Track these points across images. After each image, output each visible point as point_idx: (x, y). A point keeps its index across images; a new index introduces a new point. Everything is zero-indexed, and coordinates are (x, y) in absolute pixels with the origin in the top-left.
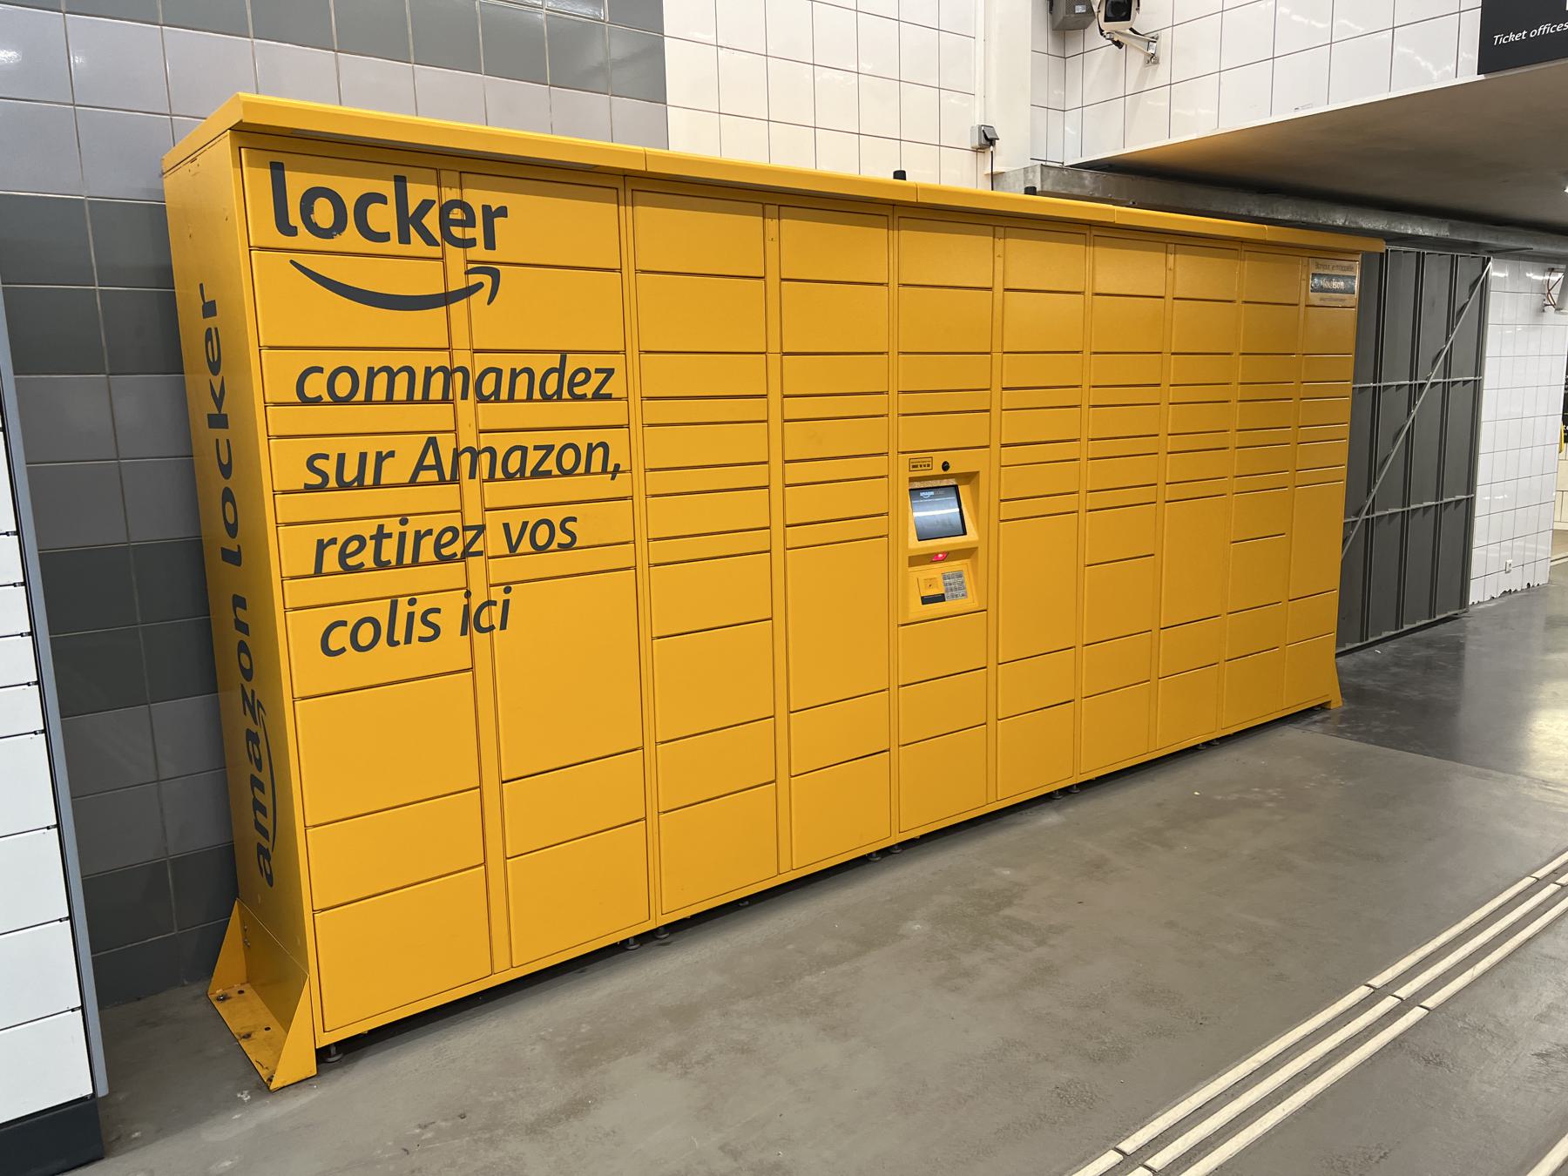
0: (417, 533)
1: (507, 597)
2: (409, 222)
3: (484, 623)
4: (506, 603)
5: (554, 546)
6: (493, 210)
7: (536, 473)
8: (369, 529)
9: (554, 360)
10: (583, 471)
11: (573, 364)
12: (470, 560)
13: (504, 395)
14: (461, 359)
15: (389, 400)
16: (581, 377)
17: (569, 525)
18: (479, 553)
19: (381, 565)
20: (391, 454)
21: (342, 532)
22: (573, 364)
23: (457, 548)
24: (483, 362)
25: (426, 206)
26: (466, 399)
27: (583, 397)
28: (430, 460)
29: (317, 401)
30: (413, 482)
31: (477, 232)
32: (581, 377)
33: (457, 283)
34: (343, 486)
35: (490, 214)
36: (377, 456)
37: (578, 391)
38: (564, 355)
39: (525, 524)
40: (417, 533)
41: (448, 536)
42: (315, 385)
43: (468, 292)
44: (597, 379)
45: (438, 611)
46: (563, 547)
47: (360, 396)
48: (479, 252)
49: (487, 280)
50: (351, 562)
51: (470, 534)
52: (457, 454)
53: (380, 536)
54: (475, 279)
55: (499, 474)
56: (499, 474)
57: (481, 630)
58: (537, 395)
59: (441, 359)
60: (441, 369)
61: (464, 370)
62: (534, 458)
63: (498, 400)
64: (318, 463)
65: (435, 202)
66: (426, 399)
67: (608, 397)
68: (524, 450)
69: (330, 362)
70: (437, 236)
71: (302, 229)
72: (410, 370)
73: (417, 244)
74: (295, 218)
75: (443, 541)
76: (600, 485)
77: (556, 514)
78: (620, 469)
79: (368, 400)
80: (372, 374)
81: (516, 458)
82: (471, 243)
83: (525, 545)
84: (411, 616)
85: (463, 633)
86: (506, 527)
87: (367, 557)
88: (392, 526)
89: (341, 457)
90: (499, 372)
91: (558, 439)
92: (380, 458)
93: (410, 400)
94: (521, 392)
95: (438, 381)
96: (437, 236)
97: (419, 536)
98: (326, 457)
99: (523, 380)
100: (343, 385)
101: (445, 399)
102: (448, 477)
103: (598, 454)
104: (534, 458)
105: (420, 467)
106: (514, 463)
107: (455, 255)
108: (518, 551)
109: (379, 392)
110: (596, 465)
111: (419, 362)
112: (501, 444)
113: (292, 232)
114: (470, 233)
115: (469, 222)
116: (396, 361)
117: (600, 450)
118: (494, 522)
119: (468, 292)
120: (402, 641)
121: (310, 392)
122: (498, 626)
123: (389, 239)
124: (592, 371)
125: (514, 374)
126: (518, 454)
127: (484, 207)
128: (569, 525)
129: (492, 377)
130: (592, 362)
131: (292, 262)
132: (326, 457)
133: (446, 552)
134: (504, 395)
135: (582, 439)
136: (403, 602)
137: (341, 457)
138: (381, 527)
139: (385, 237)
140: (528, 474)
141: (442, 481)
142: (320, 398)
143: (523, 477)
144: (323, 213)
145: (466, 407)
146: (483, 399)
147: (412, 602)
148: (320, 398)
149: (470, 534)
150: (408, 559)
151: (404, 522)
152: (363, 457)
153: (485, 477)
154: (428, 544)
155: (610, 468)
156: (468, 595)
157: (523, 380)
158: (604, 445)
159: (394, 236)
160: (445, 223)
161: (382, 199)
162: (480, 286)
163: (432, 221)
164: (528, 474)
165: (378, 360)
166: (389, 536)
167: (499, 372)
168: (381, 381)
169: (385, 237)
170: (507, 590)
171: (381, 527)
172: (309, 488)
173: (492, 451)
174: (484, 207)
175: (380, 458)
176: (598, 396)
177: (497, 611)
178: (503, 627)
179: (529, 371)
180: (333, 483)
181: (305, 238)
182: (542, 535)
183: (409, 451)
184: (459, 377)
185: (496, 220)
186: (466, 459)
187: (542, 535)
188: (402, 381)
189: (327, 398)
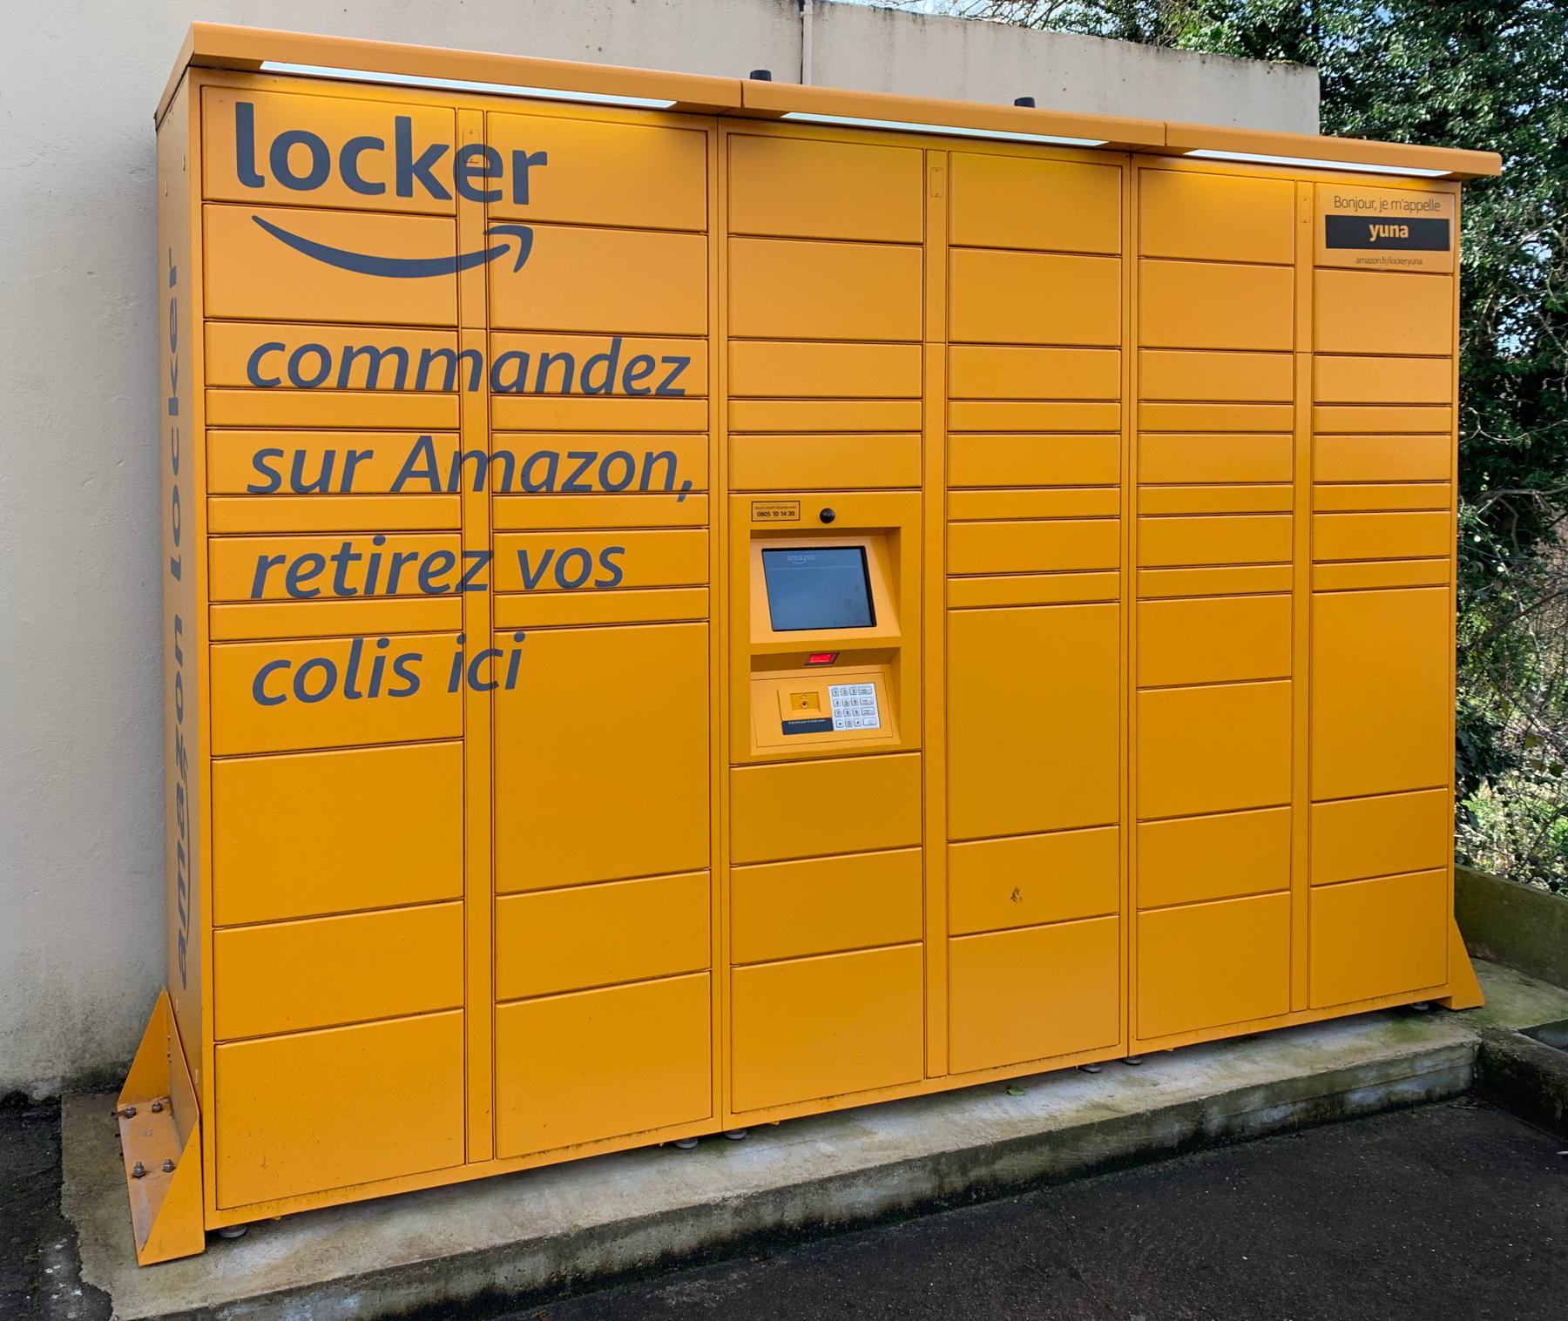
0: (397, 556)
1: (517, 646)
2: (411, 171)
3: (483, 677)
4: (516, 654)
5: (590, 583)
6: (528, 156)
7: (570, 488)
8: (329, 547)
9: (605, 345)
10: (638, 488)
11: (629, 349)
12: (469, 594)
13: (530, 385)
14: (474, 340)
15: (371, 386)
16: (640, 367)
17: (612, 558)
18: (481, 588)
19: (344, 594)
20: (368, 454)
21: (294, 548)
22: (629, 349)
23: (452, 578)
24: (503, 343)
25: (436, 151)
26: (476, 390)
27: (643, 394)
28: (421, 464)
29: (272, 385)
30: (396, 490)
32: (640, 367)
33: (473, 243)
34: (301, 491)
37: (637, 385)
38: (617, 336)
39: (549, 554)
40: (397, 556)
41: (439, 563)
42: (274, 366)
43: (487, 256)
44: (662, 371)
45: (418, 657)
46: (601, 586)
47: (332, 380)
48: (506, 208)
49: (515, 242)
50: (303, 586)
51: (471, 562)
52: (459, 459)
53: (345, 556)
54: (497, 240)
55: (516, 485)
56: (516, 485)
57: (478, 687)
58: (576, 387)
59: (448, 340)
60: (446, 352)
61: (475, 354)
62: (566, 468)
63: (520, 393)
64: (268, 461)
65: (447, 147)
66: (420, 388)
67: (679, 394)
68: (554, 457)
69: (294, 338)
70: (450, 186)
71: (270, 178)
72: (401, 353)
73: (421, 197)
74: (262, 166)
75: (432, 568)
76: (664, 508)
77: (595, 544)
78: (692, 488)
79: (342, 386)
80: (349, 354)
81: (541, 467)
82: (497, 195)
83: (548, 580)
84: (380, 661)
85: (453, 688)
86: (523, 555)
87: (324, 582)
88: (364, 545)
89: (300, 456)
90: (524, 358)
91: (603, 446)
92: (352, 459)
93: (399, 387)
94: (554, 381)
95: (438, 367)
96: (450, 186)
97: (398, 561)
98: (279, 453)
99: (557, 371)
100: (310, 367)
101: (447, 389)
102: (444, 488)
103: (661, 466)
104: (566, 468)
105: (407, 472)
106: (538, 474)
107: (472, 211)
108: (537, 587)
109: (358, 375)
110: (657, 481)
111: (414, 343)
113: (259, 182)
114: (494, 184)
115: (494, 169)
116: (382, 339)
117: (664, 462)
118: (506, 549)
119: (487, 256)
120: (365, 693)
121: (266, 371)
122: (502, 680)
123: (383, 191)
124: (658, 361)
125: (546, 361)
126: (547, 460)
127: (516, 153)
128: (612, 558)
129: (514, 363)
130: (657, 349)
131: (255, 218)
132: (279, 453)
133: (434, 582)
134: (530, 385)
135: (638, 447)
136: (370, 643)
137: (300, 456)
138: (347, 546)
139: (379, 189)
140: (557, 487)
141: (436, 490)
142: (278, 380)
143: (550, 492)
144: (300, 160)
145: (476, 400)
146: (499, 390)
147: (383, 644)
148: (278, 380)
149: (471, 562)
150: (381, 587)
151: (379, 541)
152: (329, 456)
153: (498, 487)
154: (410, 573)
155: (678, 485)
156: (462, 639)
157: (557, 371)
158: (671, 457)
160: (460, 172)
161: (378, 144)
162: (505, 248)
163: (443, 170)
164: (557, 487)
165: (358, 337)
166: (358, 557)
167: (524, 358)
168: (361, 364)
169: (379, 189)
170: (519, 638)
171: (347, 546)
172: (255, 492)
173: (509, 458)
174: (516, 153)
175: (352, 459)
176: (664, 393)
177: (503, 663)
178: (510, 685)
179: (568, 359)
180: (286, 486)
181: (273, 189)
182: (573, 570)
183: (392, 452)
184: (468, 363)
185: (532, 170)
186: (471, 466)
187: (573, 570)
188: (389, 365)
189: (286, 381)
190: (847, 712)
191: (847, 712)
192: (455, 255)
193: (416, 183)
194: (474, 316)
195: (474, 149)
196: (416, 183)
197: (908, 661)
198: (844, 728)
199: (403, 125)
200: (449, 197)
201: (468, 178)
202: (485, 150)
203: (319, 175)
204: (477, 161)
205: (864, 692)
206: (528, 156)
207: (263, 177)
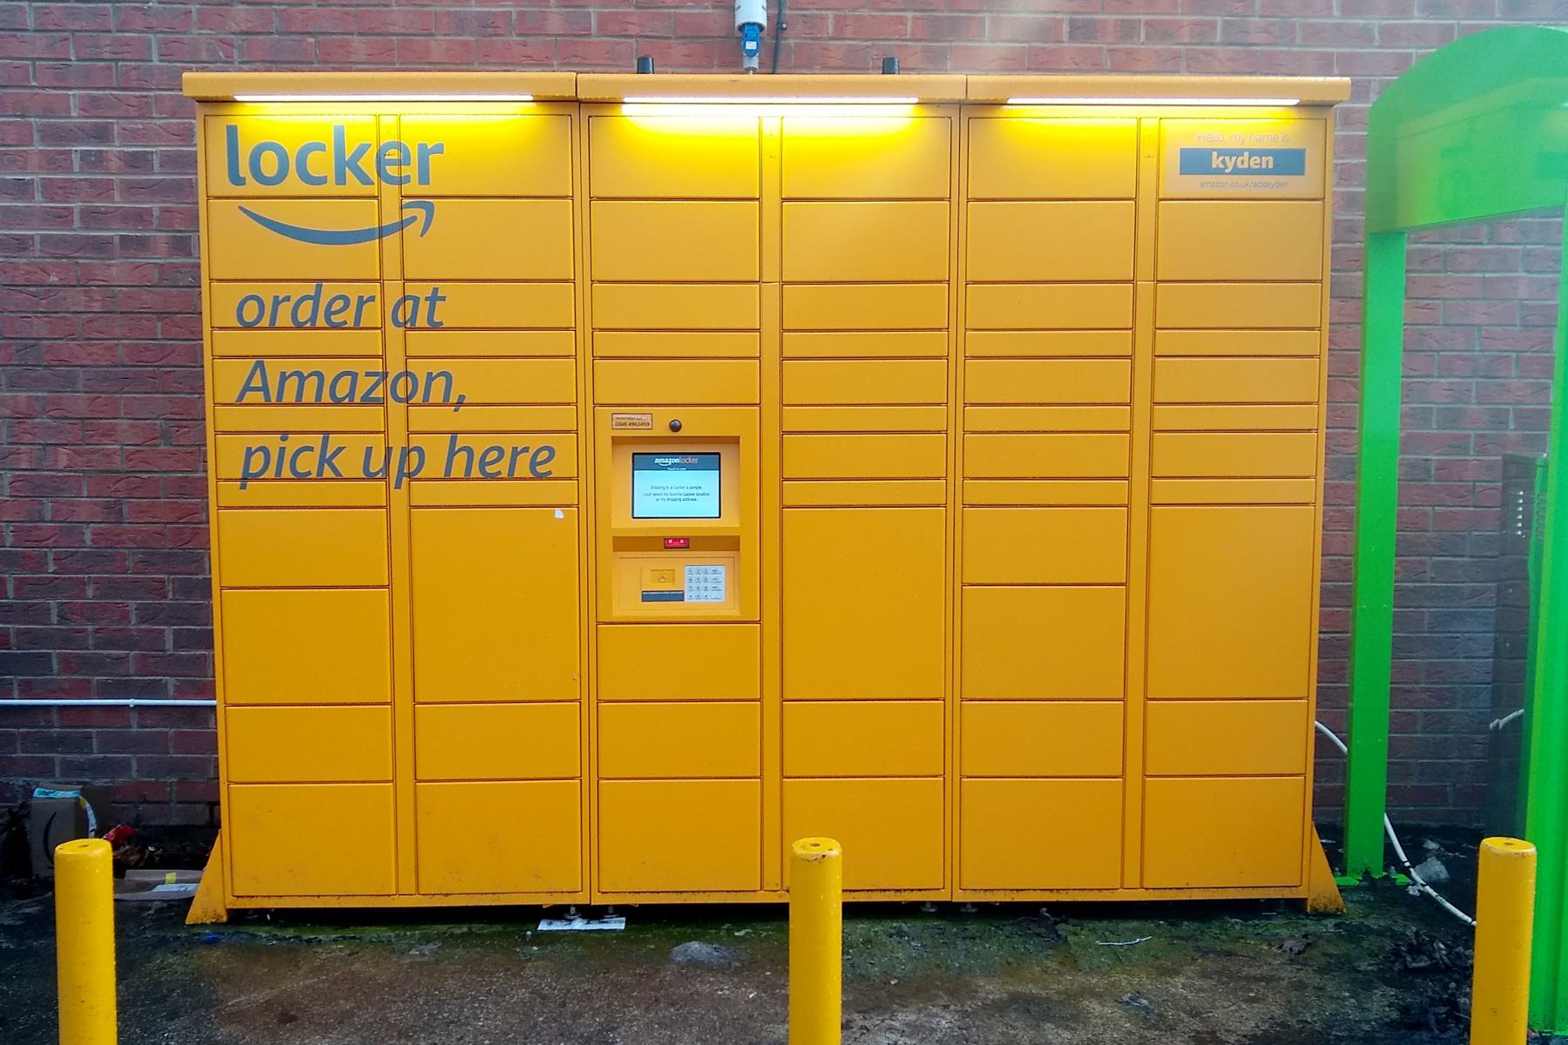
6: (429, 147)
33: (391, 218)
36: (281, 375)
42: (250, 313)
43: (401, 225)
48: (413, 188)
49: (421, 214)
54: (408, 213)
65: (370, 145)
73: (353, 185)
74: (244, 169)
96: (374, 177)
107: (390, 192)
112: (420, 369)
114: (406, 170)
119: (401, 225)
131: (241, 208)
159: (332, 179)
162: (414, 218)
169: (322, 181)
181: (252, 186)
190: (698, 588)
191: (698, 588)
192: (377, 226)
194: (392, 270)
195: (391, 145)
197: (749, 546)
198: (694, 600)
200: (373, 184)
201: (387, 167)
202: (399, 146)
203: (282, 175)
204: (393, 154)
205: (715, 572)
206: (429, 147)
207: (244, 179)
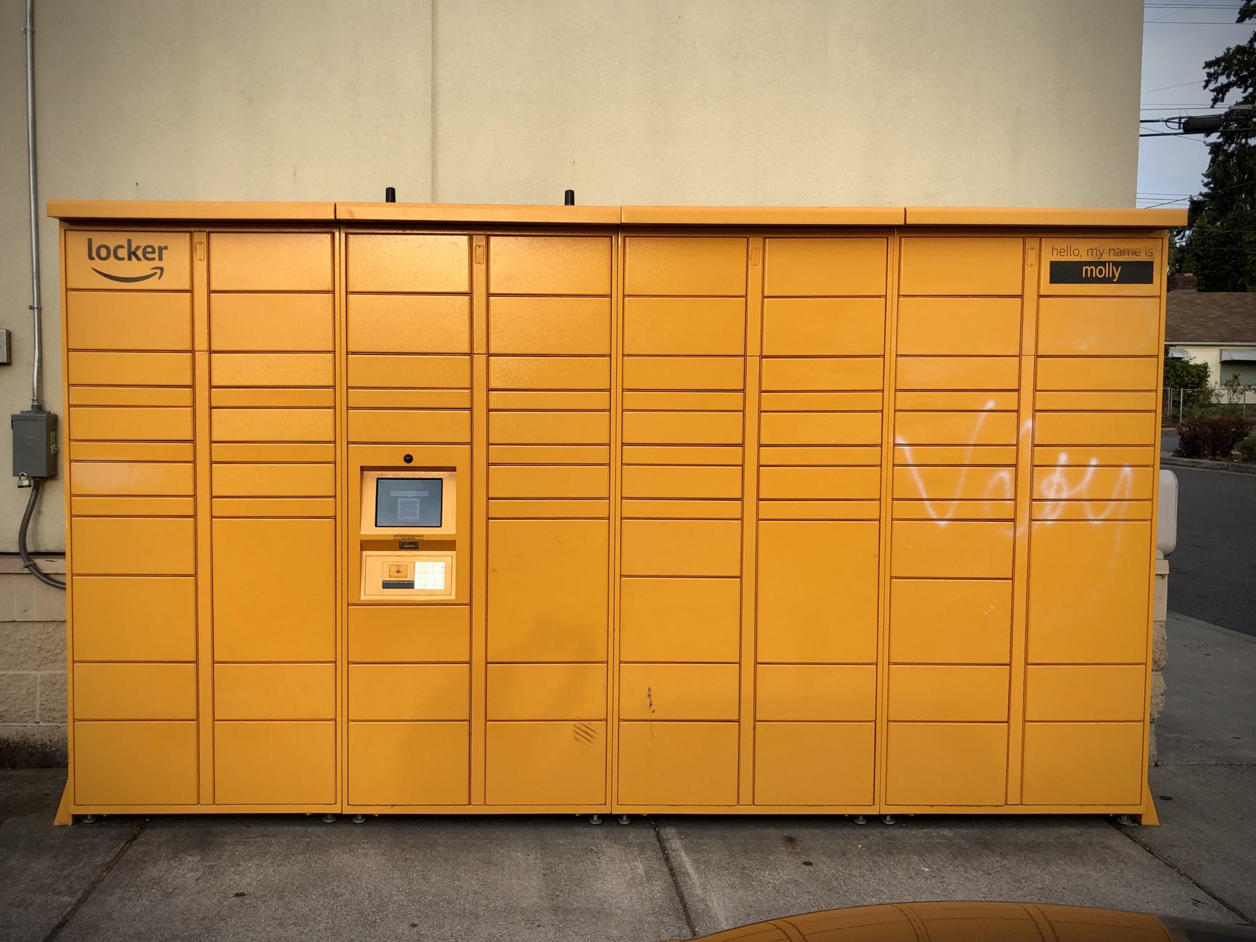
25: (138, 247)
31: (156, 255)
35: (161, 249)
49: (159, 271)
70: (141, 257)
74: (94, 255)
96: (141, 257)
113: (93, 259)
115: (153, 252)
144: (103, 253)
160: (144, 253)
161: (123, 247)
162: (156, 273)
185: (164, 251)
193: (133, 256)
196: (133, 256)
199: (129, 241)
204: (149, 250)
